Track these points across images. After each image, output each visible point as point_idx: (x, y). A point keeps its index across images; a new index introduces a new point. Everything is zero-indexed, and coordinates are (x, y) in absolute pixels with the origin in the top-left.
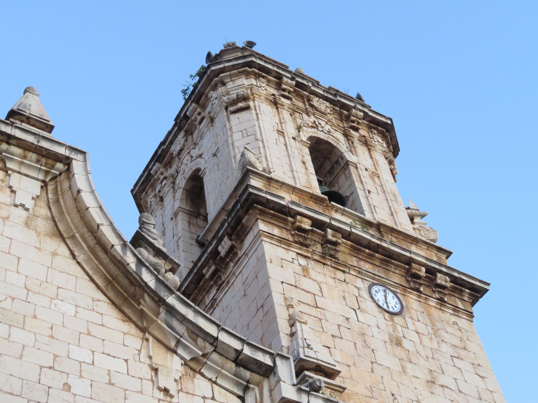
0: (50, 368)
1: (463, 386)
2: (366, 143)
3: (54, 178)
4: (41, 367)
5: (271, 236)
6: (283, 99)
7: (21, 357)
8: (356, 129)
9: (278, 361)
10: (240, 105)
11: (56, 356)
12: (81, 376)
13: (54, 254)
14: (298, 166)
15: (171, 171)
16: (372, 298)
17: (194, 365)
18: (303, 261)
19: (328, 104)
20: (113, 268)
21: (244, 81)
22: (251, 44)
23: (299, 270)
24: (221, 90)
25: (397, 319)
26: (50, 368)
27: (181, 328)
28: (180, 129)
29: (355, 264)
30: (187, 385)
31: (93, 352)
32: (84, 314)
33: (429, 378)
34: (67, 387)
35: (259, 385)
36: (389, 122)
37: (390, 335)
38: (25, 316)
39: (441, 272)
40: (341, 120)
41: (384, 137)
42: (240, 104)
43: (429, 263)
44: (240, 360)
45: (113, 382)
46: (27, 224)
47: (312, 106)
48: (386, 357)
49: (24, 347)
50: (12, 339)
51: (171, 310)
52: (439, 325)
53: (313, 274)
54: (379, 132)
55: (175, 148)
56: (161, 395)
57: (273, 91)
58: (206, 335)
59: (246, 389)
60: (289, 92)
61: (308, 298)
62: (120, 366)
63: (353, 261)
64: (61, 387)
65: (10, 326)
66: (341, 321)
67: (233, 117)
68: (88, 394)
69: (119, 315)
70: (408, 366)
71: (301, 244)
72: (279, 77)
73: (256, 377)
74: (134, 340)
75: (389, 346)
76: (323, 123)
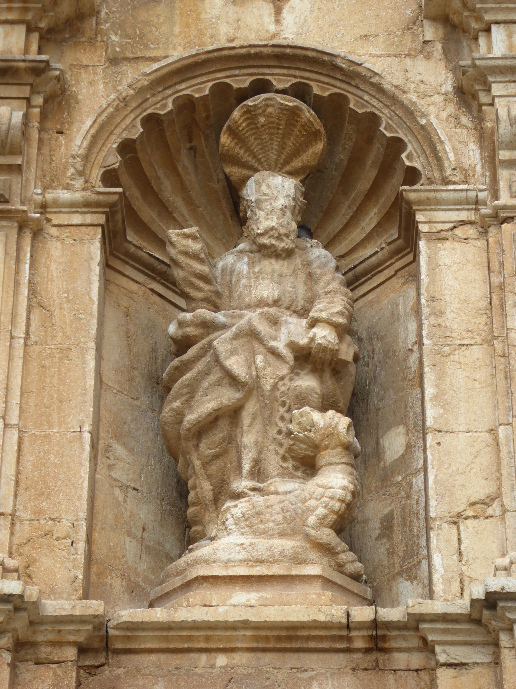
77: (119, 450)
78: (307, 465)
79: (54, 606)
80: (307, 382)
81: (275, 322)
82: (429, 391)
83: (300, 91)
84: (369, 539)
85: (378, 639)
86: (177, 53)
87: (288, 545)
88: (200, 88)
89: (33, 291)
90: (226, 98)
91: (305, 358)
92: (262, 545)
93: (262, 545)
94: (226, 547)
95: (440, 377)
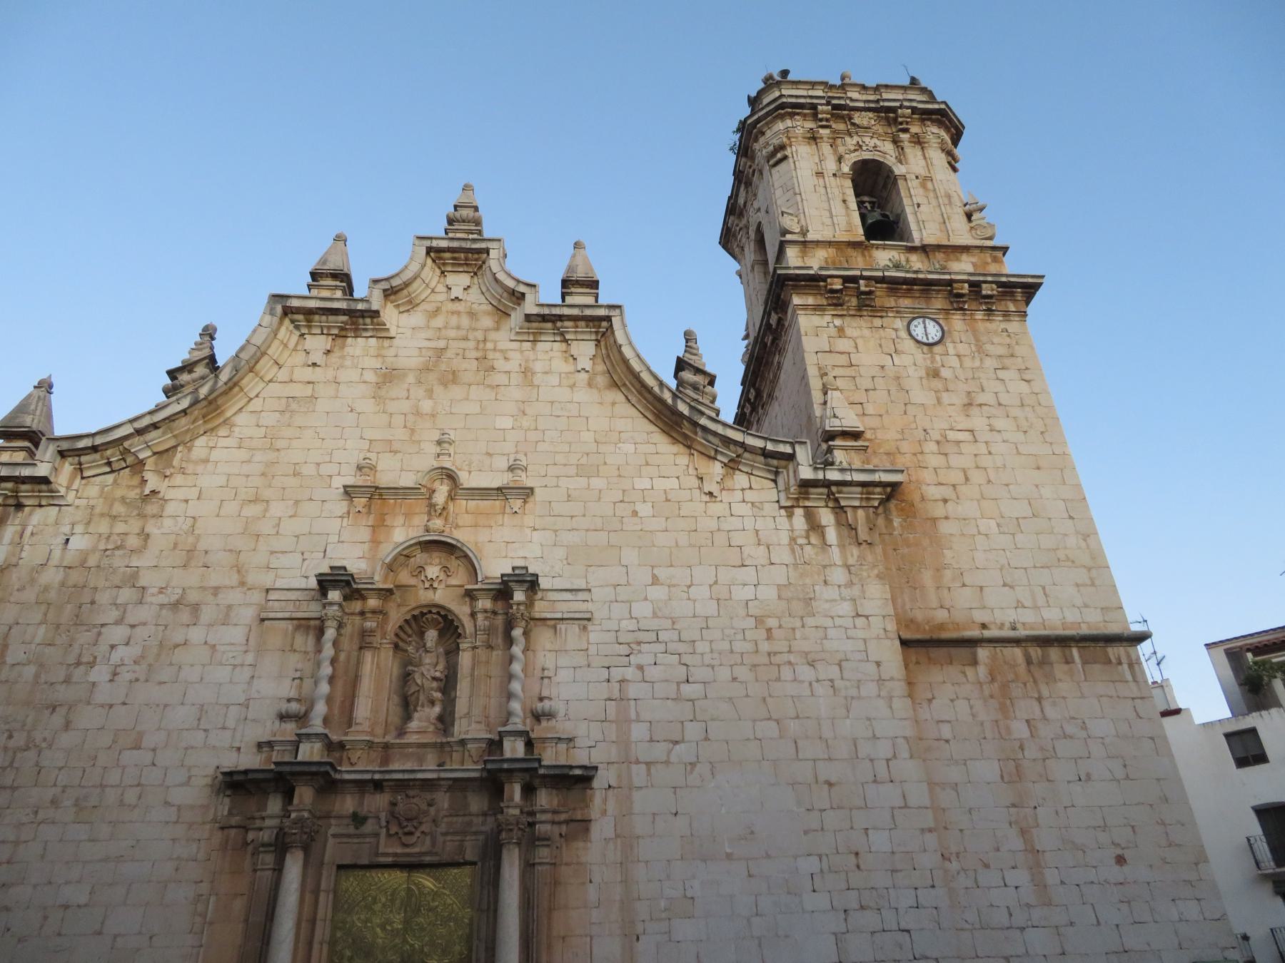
1: (1004, 398)
2: (918, 141)
3: (604, 334)
5: (805, 307)
6: (821, 131)
8: (906, 131)
9: (797, 447)
10: (779, 156)
13: (613, 404)
14: (838, 208)
15: (744, 221)
16: (910, 335)
17: (732, 465)
18: (838, 322)
19: (871, 114)
20: (658, 405)
21: (780, 126)
22: (785, 73)
23: (833, 331)
24: (762, 140)
25: (937, 349)
27: (716, 441)
28: (740, 182)
29: (893, 304)
30: (728, 483)
32: (643, 448)
33: (966, 401)
34: (635, 513)
35: (786, 467)
36: (943, 106)
37: (927, 369)
39: (986, 282)
40: (889, 125)
41: (940, 124)
42: (778, 155)
43: (972, 278)
44: (765, 453)
46: (590, 385)
47: (854, 124)
48: (920, 395)
51: (705, 429)
52: (984, 339)
53: (849, 332)
54: (933, 121)
55: (741, 201)
56: (707, 498)
57: (810, 124)
58: (736, 443)
59: (777, 473)
60: (827, 120)
61: (843, 360)
62: (673, 483)
63: (891, 302)
66: (876, 371)
67: (774, 171)
69: (670, 440)
70: (945, 396)
71: (835, 305)
72: (814, 107)
73: (783, 463)
74: (683, 460)
75: (924, 381)
76: (867, 140)
78: (432, 703)
79: (376, 740)
80: (435, 684)
83: (438, 613)
84: (445, 721)
85: (442, 745)
86: (414, 605)
87: (425, 724)
88: (416, 613)
90: (423, 614)
91: (434, 679)
94: (414, 725)
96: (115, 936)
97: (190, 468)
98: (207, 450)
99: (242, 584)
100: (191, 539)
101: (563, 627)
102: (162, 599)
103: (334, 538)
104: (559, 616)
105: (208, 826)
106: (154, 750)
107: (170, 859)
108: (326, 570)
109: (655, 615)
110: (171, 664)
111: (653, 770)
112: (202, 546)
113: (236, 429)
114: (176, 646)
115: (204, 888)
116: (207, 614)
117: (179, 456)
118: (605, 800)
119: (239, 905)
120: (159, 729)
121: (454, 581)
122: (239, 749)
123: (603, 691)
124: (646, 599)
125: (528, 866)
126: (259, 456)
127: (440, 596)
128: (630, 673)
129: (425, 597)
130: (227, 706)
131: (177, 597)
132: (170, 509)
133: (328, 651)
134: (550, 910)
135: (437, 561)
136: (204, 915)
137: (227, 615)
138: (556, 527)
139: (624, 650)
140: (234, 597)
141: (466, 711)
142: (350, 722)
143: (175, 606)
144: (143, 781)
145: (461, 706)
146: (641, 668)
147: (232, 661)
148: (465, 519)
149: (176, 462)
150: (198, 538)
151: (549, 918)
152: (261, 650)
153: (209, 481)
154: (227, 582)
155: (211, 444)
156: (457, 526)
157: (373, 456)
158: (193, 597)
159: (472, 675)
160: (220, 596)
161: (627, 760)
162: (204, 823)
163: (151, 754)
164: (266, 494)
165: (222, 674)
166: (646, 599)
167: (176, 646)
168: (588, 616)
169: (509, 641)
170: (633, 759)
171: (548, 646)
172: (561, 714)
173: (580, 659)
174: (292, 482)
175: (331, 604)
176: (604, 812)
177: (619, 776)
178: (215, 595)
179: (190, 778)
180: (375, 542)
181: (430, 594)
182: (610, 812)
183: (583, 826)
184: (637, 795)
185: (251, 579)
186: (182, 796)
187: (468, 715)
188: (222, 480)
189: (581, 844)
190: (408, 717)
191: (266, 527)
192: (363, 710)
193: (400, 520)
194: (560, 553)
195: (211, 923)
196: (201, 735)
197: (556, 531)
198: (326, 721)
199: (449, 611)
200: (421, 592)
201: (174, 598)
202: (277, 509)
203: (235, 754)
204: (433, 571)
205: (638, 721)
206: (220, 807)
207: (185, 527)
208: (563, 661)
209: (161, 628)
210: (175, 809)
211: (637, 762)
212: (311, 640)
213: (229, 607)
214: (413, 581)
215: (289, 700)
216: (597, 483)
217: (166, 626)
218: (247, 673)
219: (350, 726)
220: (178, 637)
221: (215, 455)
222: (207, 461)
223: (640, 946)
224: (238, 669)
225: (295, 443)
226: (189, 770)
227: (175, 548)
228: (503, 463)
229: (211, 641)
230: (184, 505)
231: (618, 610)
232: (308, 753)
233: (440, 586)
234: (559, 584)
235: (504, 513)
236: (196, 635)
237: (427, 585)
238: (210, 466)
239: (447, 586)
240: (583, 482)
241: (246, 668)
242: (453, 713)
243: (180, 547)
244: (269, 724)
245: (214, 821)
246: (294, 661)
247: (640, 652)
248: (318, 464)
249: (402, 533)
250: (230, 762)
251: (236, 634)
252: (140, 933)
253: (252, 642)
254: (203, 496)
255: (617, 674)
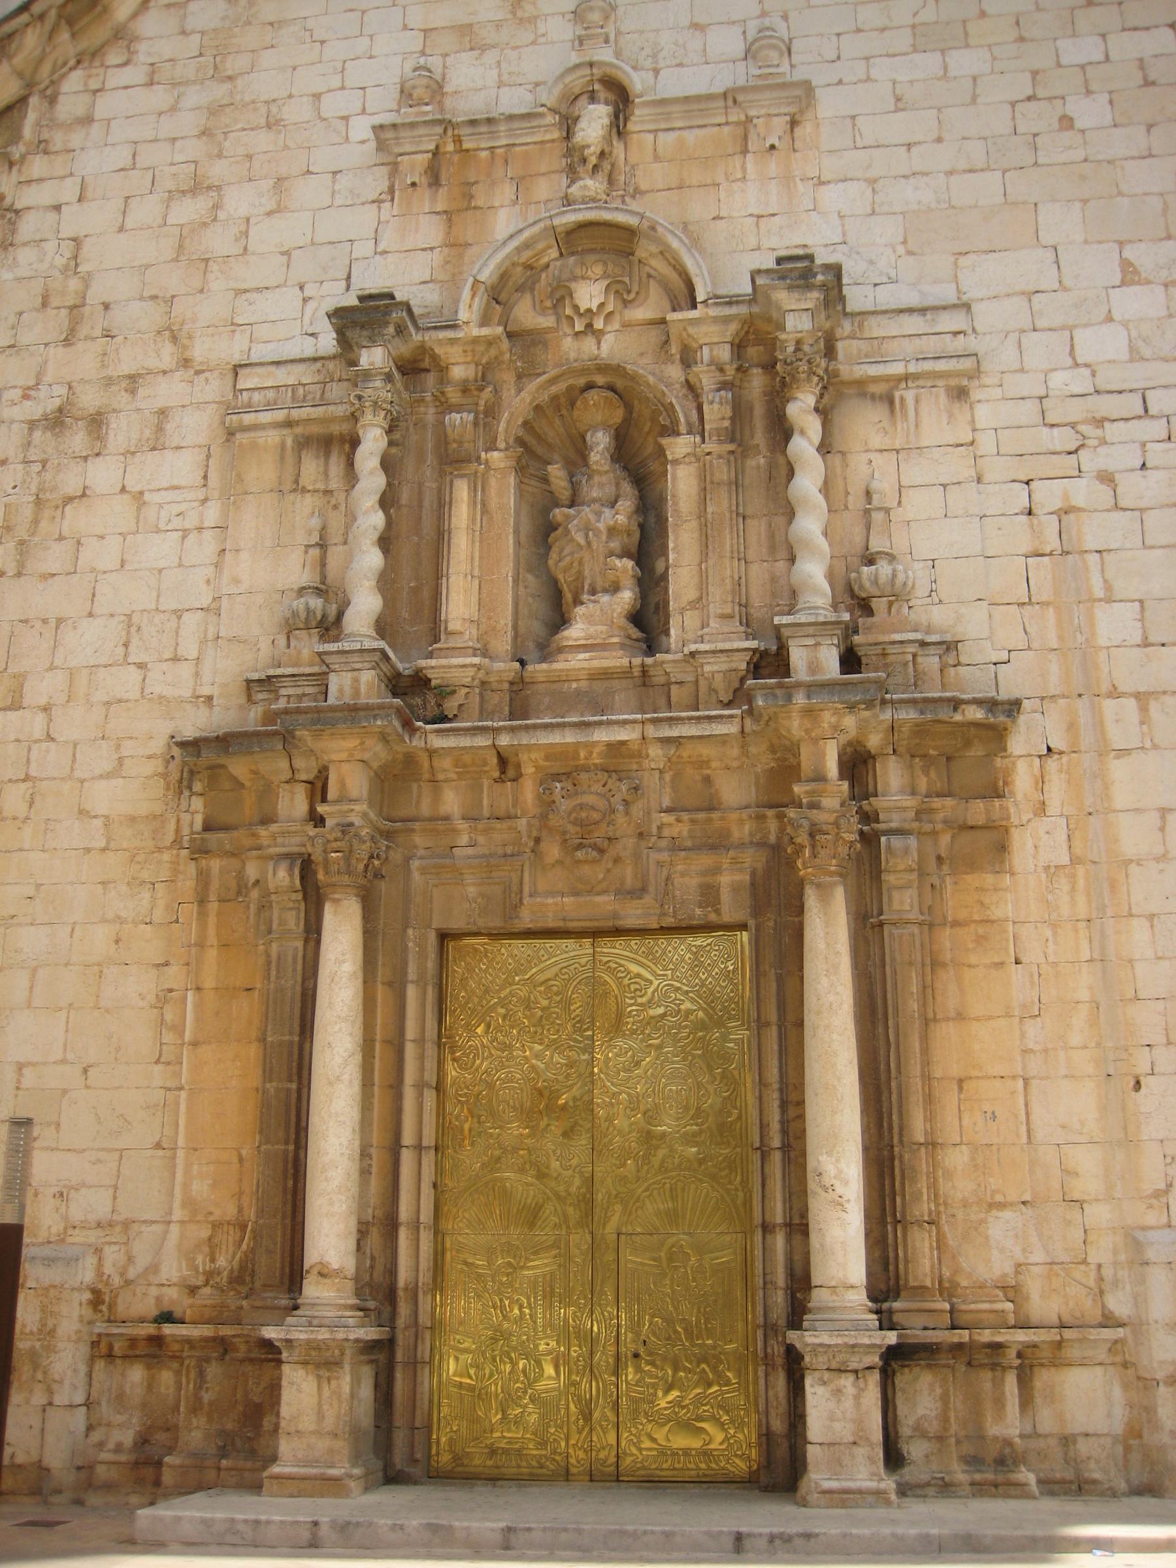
0: (1029, 99)
4: (1013, 104)
7: (974, 99)
11: (1035, 73)
12: (1089, 92)
26: (1029, 99)
31: (1103, 36)
34: (1067, 122)
38: (964, 22)
45: (1151, 79)
49: (975, 79)
50: (951, 74)
64: (1056, 125)
65: (943, 52)
68: (1108, 120)
77: (530, 577)
81: (598, 514)
82: (671, 545)
89: (484, 504)
92: (592, 629)
93: (592, 629)
94: (575, 632)
95: (676, 538)
96: (20, 1067)
97: (58, 139)
98: (86, 98)
99: (186, 363)
100: (74, 284)
101: (909, 396)
102: (32, 409)
103: (364, 249)
104: (897, 369)
105: (166, 856)
106: (46, 709)
107: (104, 920)
108: (351, 301)
109: (1135, 355)
110: (61, 538)
111: (1153, 706)
112: (95, 295)
113: (142, 47)
114: (69, 500)
115: (175, 976)
116: (123, 430)
117: (31, 116)
118: (1041, 781)
119: (246, 1010)
120: (52, 668)
121: (640, 313)
122: (210, 698)
123: (1018, 534)
124: (1109, 319)
125: (868, 928)
126: (194, 97)
127: (612, 346)
128: (1082, 492)
129: (574, 349)
130: (178, 614)
131: (57, 402)
132: (28, 227)
133: (372, 480)
134: (927, 1022)
135: (598, 270)
136: (178, 1029)
137: (160, 429)
138: (872, 174)
139: (1063, 439)
140: (168, 391)
141: (691, 594)
142: (435, 629)
143: (57, 421)
144: (33, 773)
145: (681, 583)
146: (1107, 478)
147: (177, 523)
148: (652, 175)
149: (27, 131)
150: (87, 280)
151: (925, 1038)
152: (234, 492)
153: (97, 159)
154: (152, 363)
155: (94, 84)
156: (637, 192)
157: (435, 62)
158: (89, 399)
159: (702, 514)
160: (141, 392)
161: (1092, 690)
162: (159, 850)
163: (41, 718)
164: (218, 171)
165: (160, 550)
166: (1109, 319)
167: (69, 500)
168: (968, 364)
169: (782, 431)
170: (1105, 687)
171: (877, 441)
172: (921, 591)
173: (957, 466)
174: (262, 141)
175: (367, 375)
176: (1041, 809)
177: (1072, 727)
178: (133, 392)
179: (120, 760)
180: (456, 246)
181: (588, 345)
182: (1053, 808)
183: (993, 845)
184: (1118, 769)
185: (199, 351)
186: (107, 797)
187: (699, 603)
188: (122, 156)
189: (989, 879)
190: (559, 619)
191: (219, 242)
192: (459, 605)
193: (507, 191)
194: (888, 230)
195: (195, 1044)
196: (134, 675)
197: (872, 182)
198: (382, 627)
199: (633, 378)
200: (568, 343)
201: (53, 404)
202: (240, 201)
203: (203, 711)
204: (589, 294)
205: (1109, 600)
206: (186, 818)
207: (60, 261)
208: (914, 472)
209: (37, 467)
210: (98, 823)
211: (1115, 693)
212: (336, 466)
213: (163, 413)
214: (547, 321)
215: (301, 591)
216: (964, 62)
217: (44, 463)
218: (208, 545)
219: (436, 639)
220: (71, 483)
221: (104, 106)
222: (87, 120)
223: (1145, 1100)
224: (192, 538)
225: (268, 58)
226: (118, 747)
227: (45, 305)
228: (729, 43)
229: (133, 485)
230: (52, 216)
231: (1041, 350)
232: (348, 690)
233: (608, 330)
234: (886, 297)
235: (745, 151)
236: (103, 474)
237: (579, 326)
238: (96, 130)
239: (626, 325)
240: (930, 62)
241: (208, 535)
242: (662, 608)
243: (55, 301)
244: (264, 645)
245: (177, 842)
246: (304, 513)
247: (1103, 442)
248: (317, 97)
249: (508, 224)
250: (195, 723)
251: (181, 467)
252: (64, 1061)
253: (213, 476)
254: (89, 194)
255: (1049, 495)
